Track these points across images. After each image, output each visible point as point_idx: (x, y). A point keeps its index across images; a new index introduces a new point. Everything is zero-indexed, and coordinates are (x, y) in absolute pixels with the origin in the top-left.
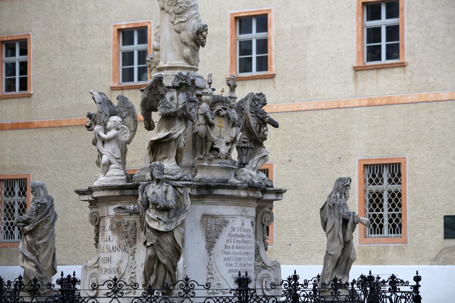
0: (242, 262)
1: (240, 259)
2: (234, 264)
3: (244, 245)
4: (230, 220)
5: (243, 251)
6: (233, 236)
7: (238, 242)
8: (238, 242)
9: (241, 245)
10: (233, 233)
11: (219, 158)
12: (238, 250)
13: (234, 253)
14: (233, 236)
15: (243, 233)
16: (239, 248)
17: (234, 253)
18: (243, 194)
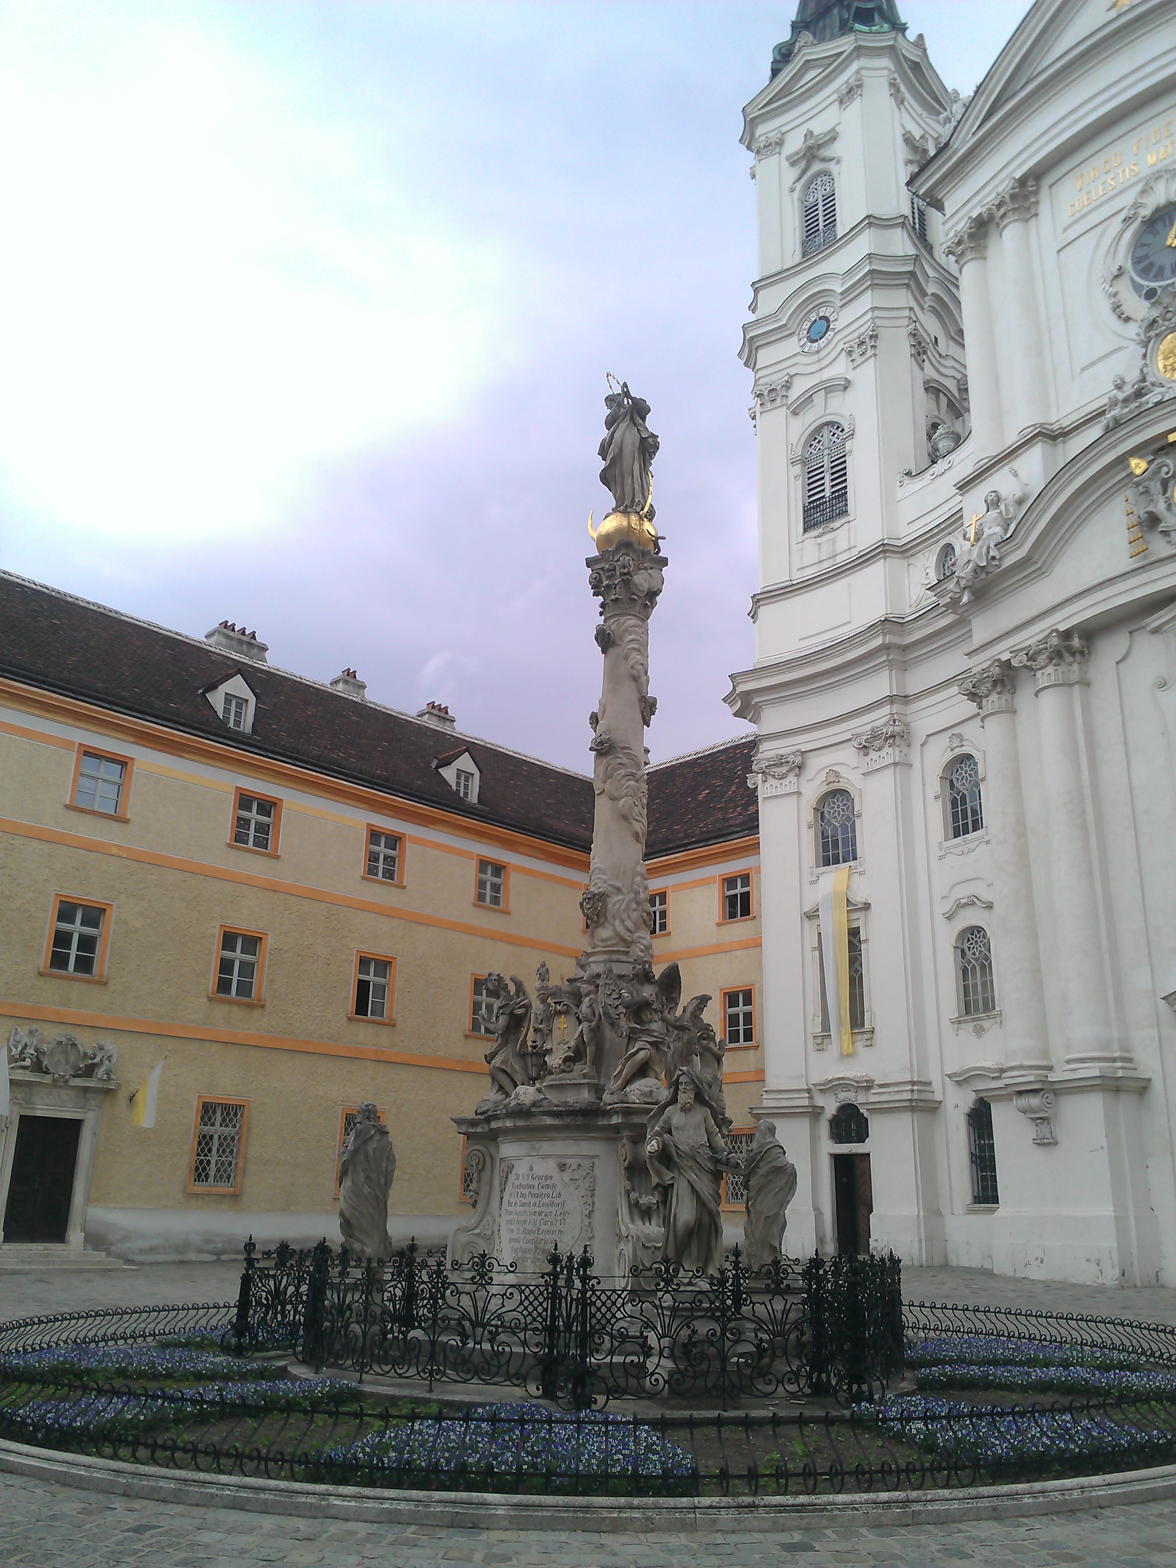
0: (527, 1226)
1: (524, 1222)
2: (515, 1230)
3: (533, 1200)
4: (515, 1163)
5: (528, 1209)
6: (517, 1187)
7: (523, 1196)
8: (523, 1196)
9: (527, 1200)
10: (517, 1183)
11: (551, 1073)
12: (522, 1209)
13: (516, 1214)
14: (517, 1187)
15: (531, 1182)
16: (523, 1205)
17: (516, 1214)
18: (509, 1123)
